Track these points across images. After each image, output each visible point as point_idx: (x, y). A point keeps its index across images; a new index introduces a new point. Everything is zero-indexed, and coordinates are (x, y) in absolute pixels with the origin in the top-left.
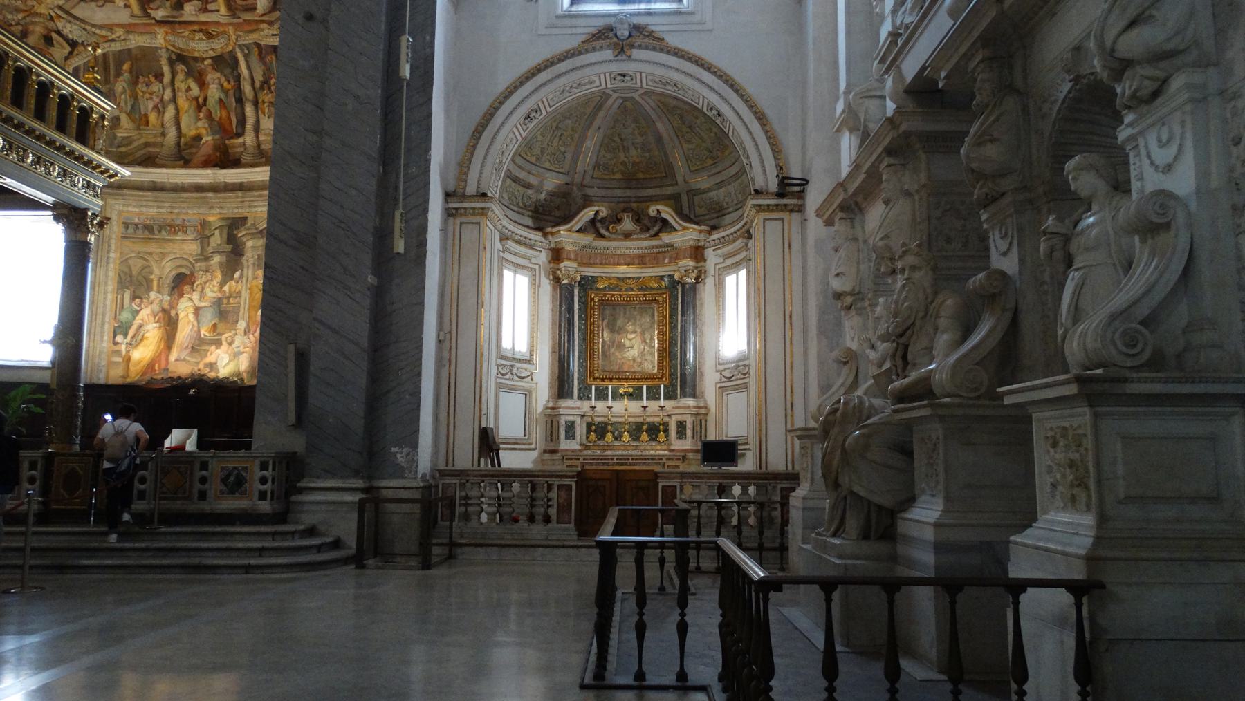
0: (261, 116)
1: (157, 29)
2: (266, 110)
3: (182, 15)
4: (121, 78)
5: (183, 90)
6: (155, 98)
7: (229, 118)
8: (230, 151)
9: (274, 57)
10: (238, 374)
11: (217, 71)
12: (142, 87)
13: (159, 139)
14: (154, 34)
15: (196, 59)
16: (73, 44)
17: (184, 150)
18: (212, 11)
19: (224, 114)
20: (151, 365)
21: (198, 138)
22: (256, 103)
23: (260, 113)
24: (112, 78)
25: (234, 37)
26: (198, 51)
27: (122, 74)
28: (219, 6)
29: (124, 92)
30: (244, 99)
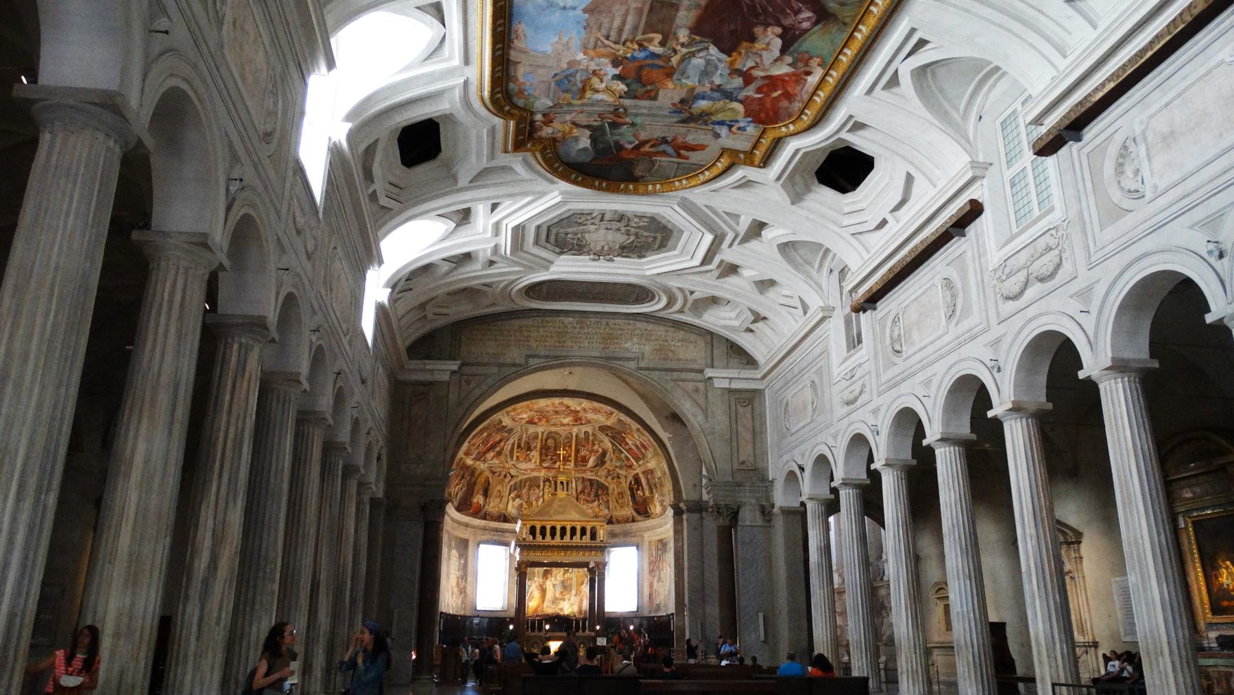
10: (573, 613)
16: (512, 477)
20: (536, 610)
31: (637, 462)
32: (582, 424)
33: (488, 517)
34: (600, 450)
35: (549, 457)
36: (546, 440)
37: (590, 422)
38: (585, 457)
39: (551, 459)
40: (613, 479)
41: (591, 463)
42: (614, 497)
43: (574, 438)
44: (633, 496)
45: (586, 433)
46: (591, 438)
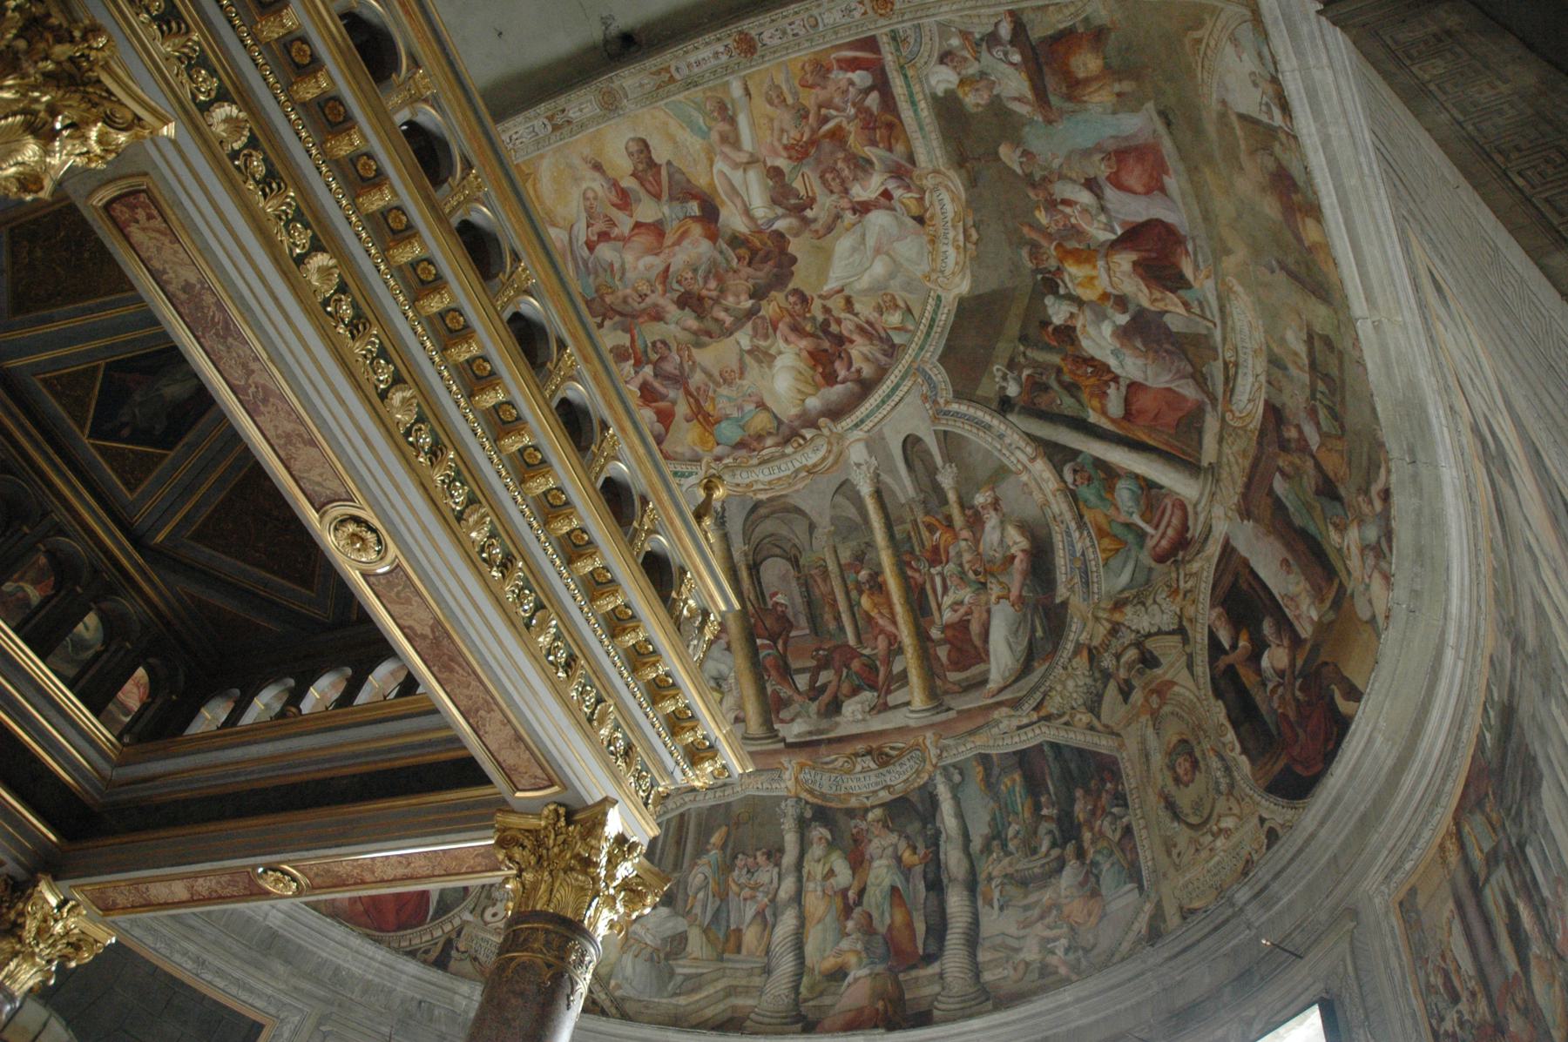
0: (983, 909)
1: (784, 760)
2: (996, 895)
3: (837, 724)
4: (705, 859)
5: (819, 877)
6: (760, 896)
7: (910, 925)
8: (907, 996)
9: (1017, 777)
11: (892, 831)
12: (740, 876)
13: (757, 981)
14: (780, 770)
15: (851, 813)
17: (806, 1000)
18: (896, 707)
19: (899, 918)
21: (839, 974)
22: (972, 886)
23: (980, 902)
24: (685, 866)
25: (933, 752)
26: (858, 795)
27: (708, 851)
28: (912, 693)
29: (705, 886)
30: (945, 881)
31: (1191, 466)
32: (866, 387)
33: (453, 964)
34: (1018, 542)
35: (802, 681)
36: (754, 568)
37: (892, 350)
38: (963, 625)
39: (815, 692)
40: (1126, 692)
41: (1002, 656)
42: (1152, 798)
43: (871, 506)
44: (1244, 713)
45: (911, 444)
46: (946, 480)
